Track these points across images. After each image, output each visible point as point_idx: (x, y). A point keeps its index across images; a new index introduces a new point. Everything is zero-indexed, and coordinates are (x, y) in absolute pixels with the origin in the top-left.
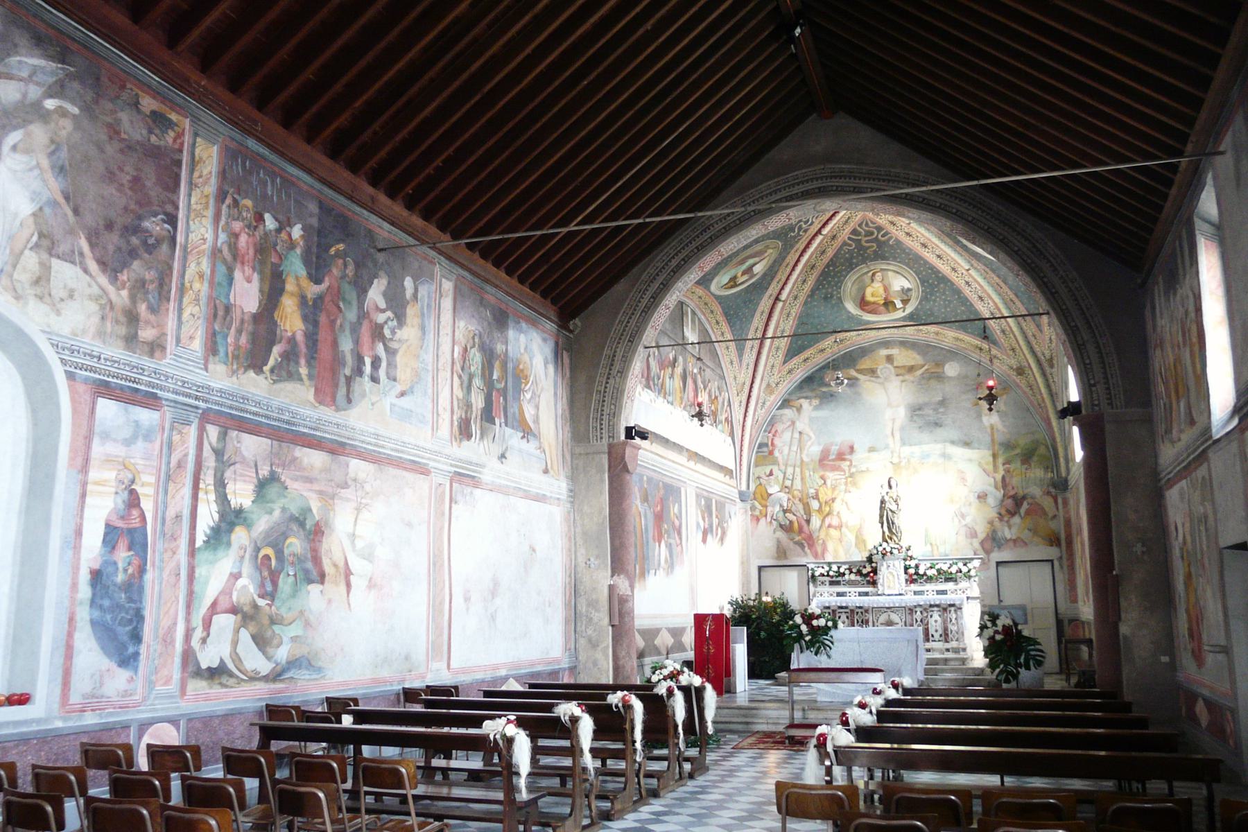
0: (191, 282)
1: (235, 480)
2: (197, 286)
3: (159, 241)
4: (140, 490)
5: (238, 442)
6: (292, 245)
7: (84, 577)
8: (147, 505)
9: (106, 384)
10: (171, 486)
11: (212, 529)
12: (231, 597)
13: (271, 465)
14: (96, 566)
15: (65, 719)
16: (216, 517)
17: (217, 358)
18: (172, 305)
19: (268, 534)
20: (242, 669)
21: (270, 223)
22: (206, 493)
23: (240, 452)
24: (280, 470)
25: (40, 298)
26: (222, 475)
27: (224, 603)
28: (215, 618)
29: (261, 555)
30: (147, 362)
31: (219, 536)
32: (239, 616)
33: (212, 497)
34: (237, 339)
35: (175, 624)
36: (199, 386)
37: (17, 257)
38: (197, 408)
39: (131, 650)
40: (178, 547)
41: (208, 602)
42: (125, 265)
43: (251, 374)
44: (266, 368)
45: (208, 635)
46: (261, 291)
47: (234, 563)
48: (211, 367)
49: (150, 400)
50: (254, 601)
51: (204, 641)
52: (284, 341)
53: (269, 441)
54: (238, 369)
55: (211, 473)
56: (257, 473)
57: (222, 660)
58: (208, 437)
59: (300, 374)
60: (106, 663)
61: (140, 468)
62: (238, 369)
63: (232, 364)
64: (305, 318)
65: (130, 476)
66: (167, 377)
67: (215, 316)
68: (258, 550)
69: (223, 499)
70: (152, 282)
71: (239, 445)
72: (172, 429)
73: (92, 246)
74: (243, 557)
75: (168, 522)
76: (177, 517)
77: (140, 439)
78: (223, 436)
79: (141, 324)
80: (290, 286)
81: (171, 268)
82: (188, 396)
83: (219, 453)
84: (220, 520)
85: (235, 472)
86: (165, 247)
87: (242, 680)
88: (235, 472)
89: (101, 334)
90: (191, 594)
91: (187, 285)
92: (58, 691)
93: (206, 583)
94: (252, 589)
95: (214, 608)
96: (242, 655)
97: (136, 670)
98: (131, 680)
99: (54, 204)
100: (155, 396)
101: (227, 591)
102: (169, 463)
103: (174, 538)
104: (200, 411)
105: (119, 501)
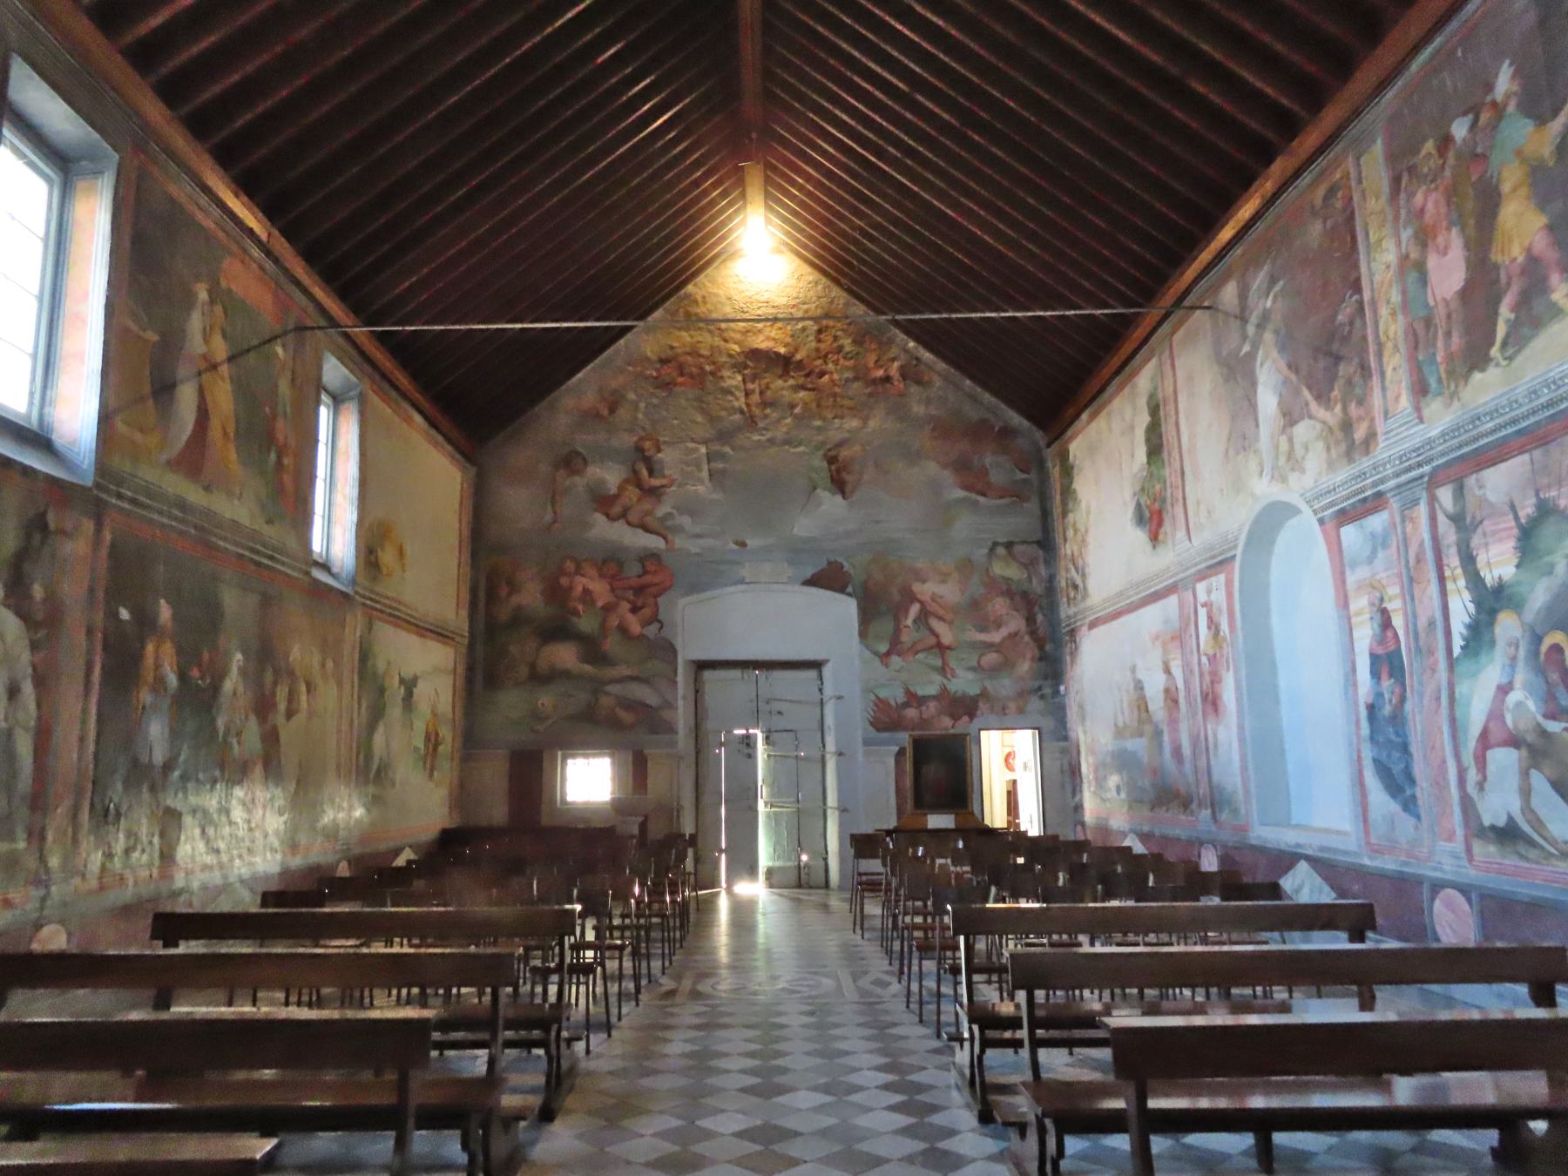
0: (1386, 332)
1: (1486, 545)
2: (1392, 328)
3: (1351, 323)
4: (1389, 606)
5: (1481, 487)
6: (1498, 109)
7: (1363, 713)
8: (1398, 622)
9: (1342, 512)
10: (1416, 592)
11: (1469, 627)
12: (1504, 722)
13: (1537, 494)
14: (1370, 701)
15: (1370, 858)
16: (1471, 608)
17: (1430, 396)
18: (1375, 381)
19: (1550, 609)
20: (1545, 833)
21: (1460, 130)
22: (1455, 580)
23: (1486, 500)
24: (1553, 493)
25: (1293, 469)
26: (1468, 546)
27: (1496, 734)
28: (1490, 754)
29: (1544, 648)
30: (1365, 463)
31: (1480, 633)
32: (1524, 752)
33: (1462, 583)
34: (1447, 345)
35: (1444, 761)
36: (1418, 449)
37: (1277, 447)
38: (1422, 477)
39: (1408, 792)
40: (1436, 662)
41: (1475, 730)
42: (1332, 379)
43: (1477, 376)
44: (1495, 351)
45: (1485, 778)
46: (1467, 246)
47: (1503, 668)
48: (1426, 412)
49: (1375, 503)
50: (1539, 725)
51: (1481, 786)
52: (1515, 279)
53: (1526, 457)
54: (1457, 386)
55: (1453, 550)
56: (1517, 518)
57: (1510, 818)
58: (1441, 506)
59: (1554, 304)
60: (1394, 807)
61: (1384, 582)
62: (1457, 386)
63: (1449, 387)
64: (1542, 203)
65: (1378, 595)
66: (1384, 464)
67: (1416, 348)
68: (1537, 639)
69: (1475, 580)
70: (1355, 372)
71: (1481, 492)
72: (1403, 521)
73: (1310, 388)
74: (1514, 659)
75: (1422, 635)
76: (1430, 625)
77: (1379, 548)
78: (1460, 493)
79: (1355, 426)
80: (1511, 177)
81: (1364, 338)
82: (1409, 469)
83: (1457, 519)
84: (1478, 612)
85: (1485, 535)
86: (1358, 323)
87: (1552, 855)
88: (1485, 535)
89: (1331, 466)
90: (1453, 721)
91: (1383, 338)
92: (1361, 826)
93: (1468, 705)
94: (1531, 705)
95: (1485, 742)
96: (1543, 813)
97: (1418, 817)
98: (1416, 828)
99: (1286, 381)
100: (1379, 495)
101: (1496, 714)
102: (1408, 562)
103: (1431, 652)
104: (1426, 479)
105: (1376, 626)
